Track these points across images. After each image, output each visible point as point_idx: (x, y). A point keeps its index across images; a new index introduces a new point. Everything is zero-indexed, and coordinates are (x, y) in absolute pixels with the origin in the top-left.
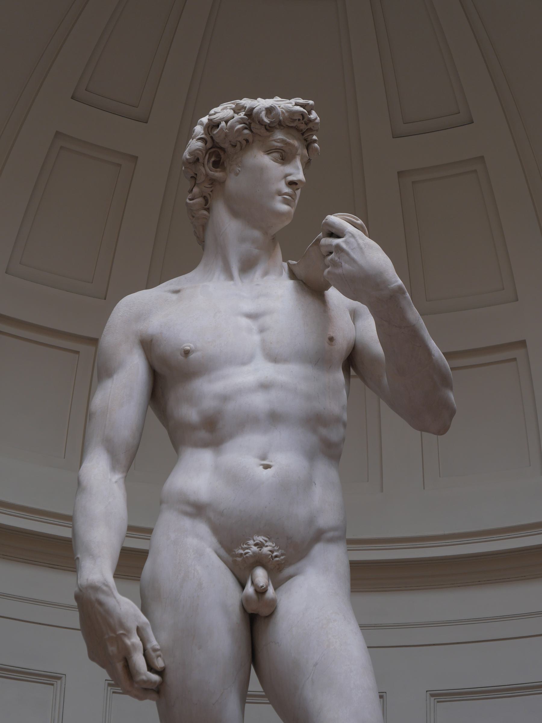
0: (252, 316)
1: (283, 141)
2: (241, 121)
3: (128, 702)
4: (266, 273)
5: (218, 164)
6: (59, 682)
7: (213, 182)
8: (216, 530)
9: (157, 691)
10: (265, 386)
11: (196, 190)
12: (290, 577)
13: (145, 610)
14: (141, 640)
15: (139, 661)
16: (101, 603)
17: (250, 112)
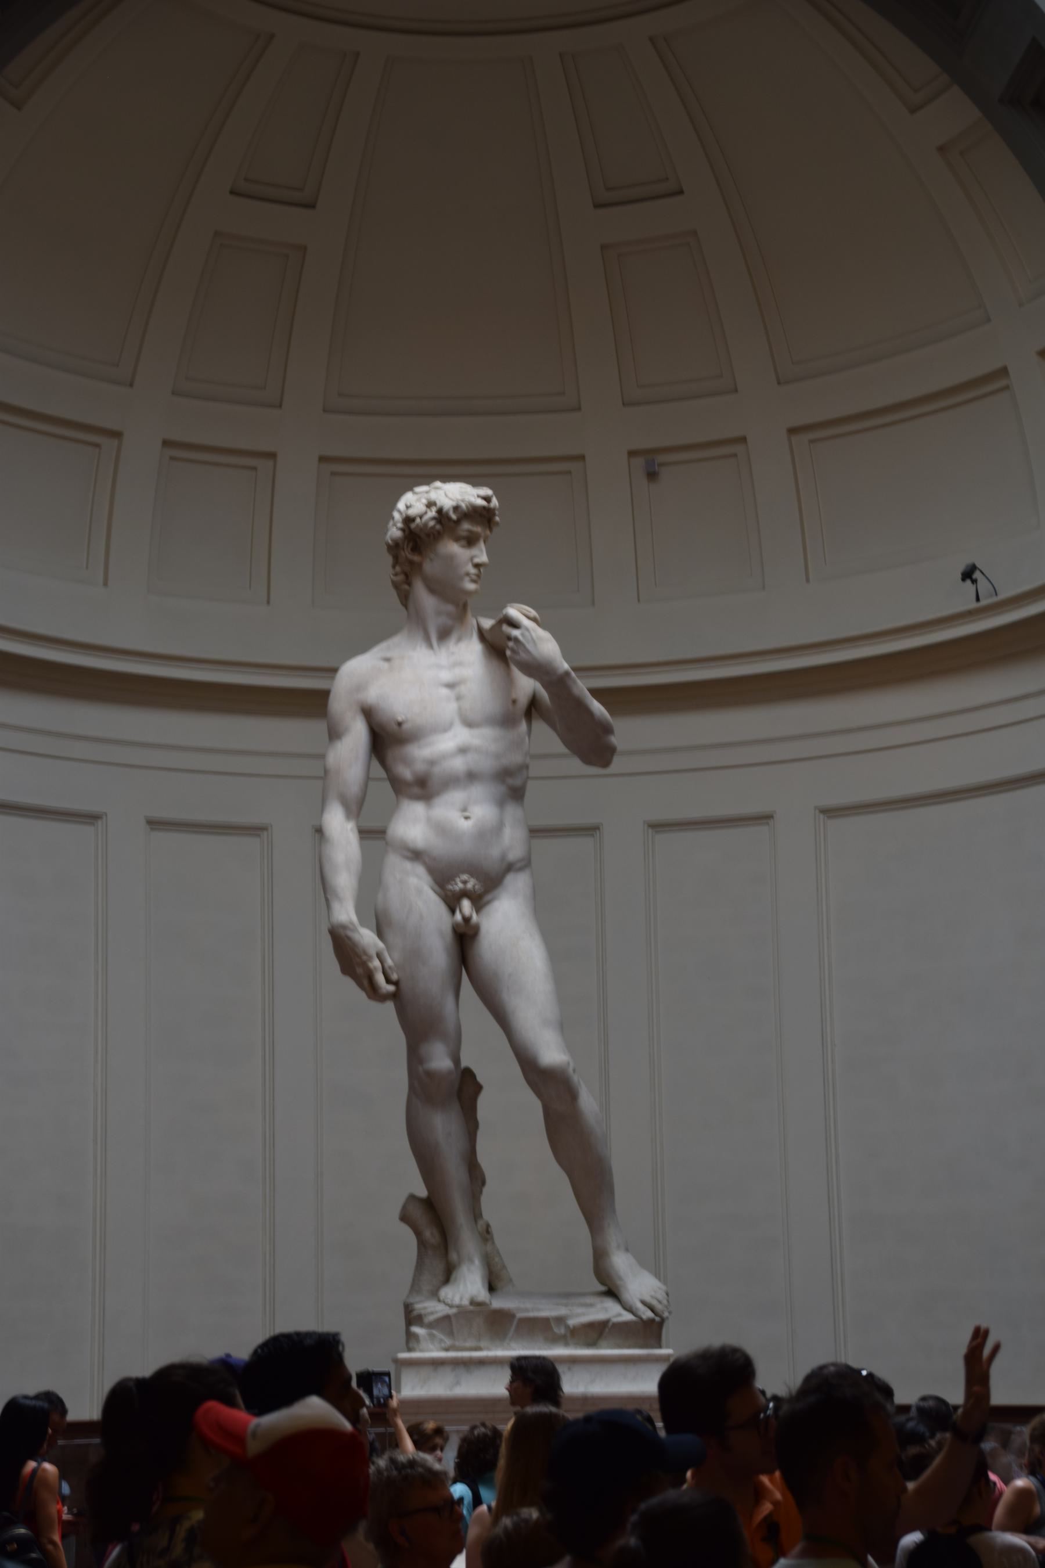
0: (450, 686)
1: (470, 531)
2: (434, 518)
3: (374, 1005)
4: (459, 640)
5: (416, 549)
6: (265, 833)
7: (411, 563)
8: (431, 871)
9: (395, 996)
10: (463, 750)
11: (398, 569)
12: (488, 902)
13: (380, 934)
14: (382, 962)
15: (380, 978)
16: (349, 938)
17: (440, 511)
